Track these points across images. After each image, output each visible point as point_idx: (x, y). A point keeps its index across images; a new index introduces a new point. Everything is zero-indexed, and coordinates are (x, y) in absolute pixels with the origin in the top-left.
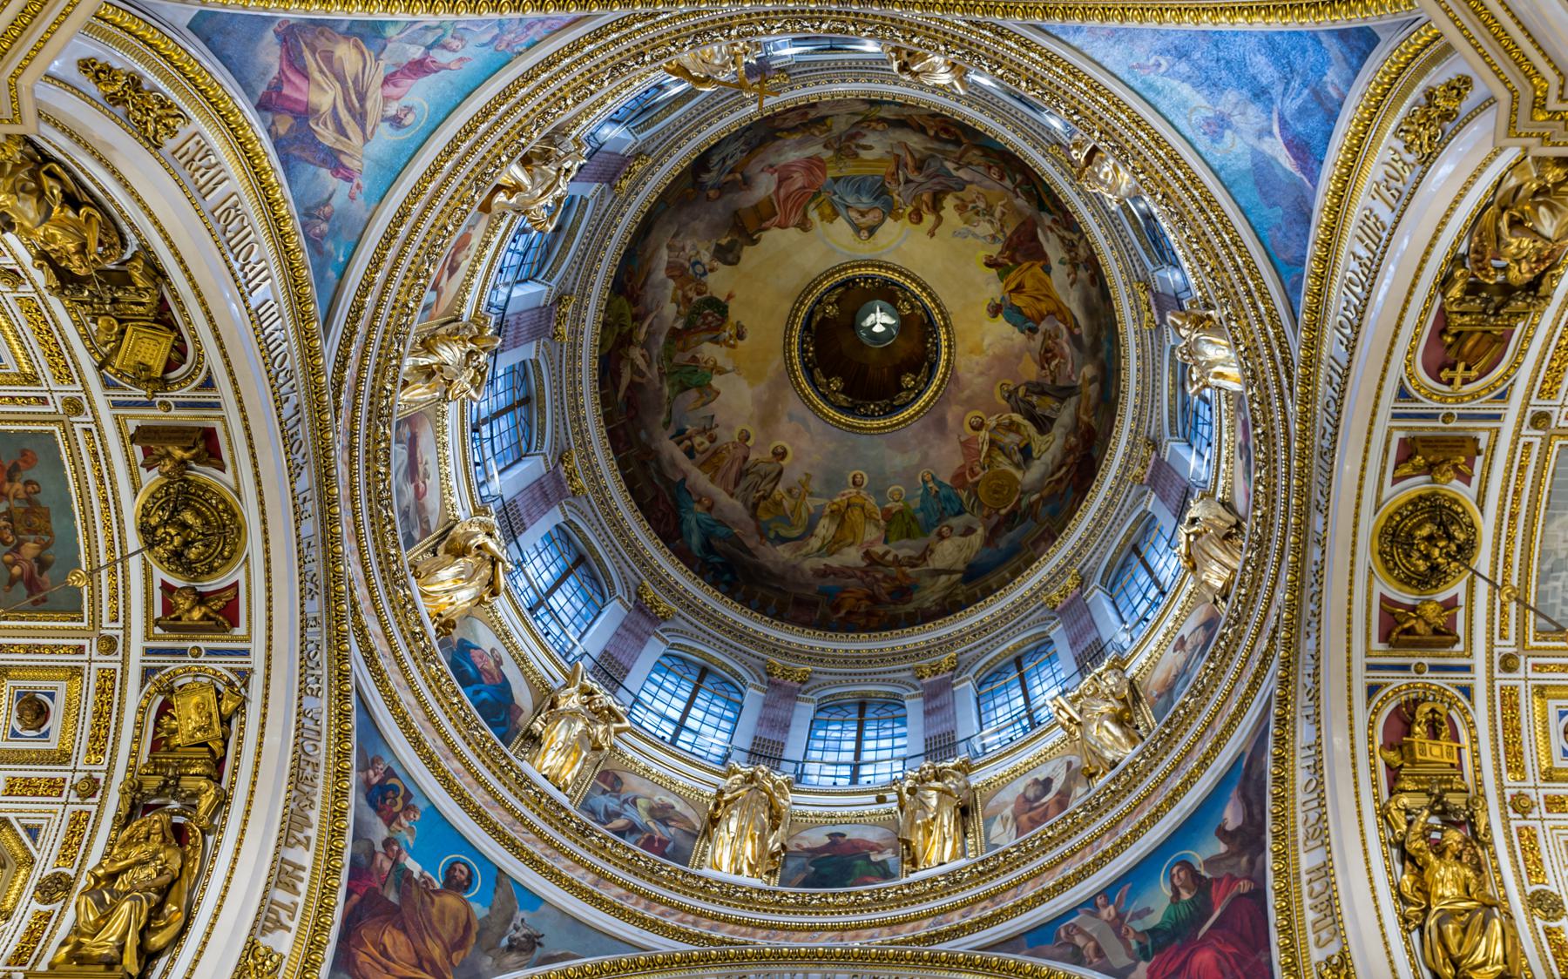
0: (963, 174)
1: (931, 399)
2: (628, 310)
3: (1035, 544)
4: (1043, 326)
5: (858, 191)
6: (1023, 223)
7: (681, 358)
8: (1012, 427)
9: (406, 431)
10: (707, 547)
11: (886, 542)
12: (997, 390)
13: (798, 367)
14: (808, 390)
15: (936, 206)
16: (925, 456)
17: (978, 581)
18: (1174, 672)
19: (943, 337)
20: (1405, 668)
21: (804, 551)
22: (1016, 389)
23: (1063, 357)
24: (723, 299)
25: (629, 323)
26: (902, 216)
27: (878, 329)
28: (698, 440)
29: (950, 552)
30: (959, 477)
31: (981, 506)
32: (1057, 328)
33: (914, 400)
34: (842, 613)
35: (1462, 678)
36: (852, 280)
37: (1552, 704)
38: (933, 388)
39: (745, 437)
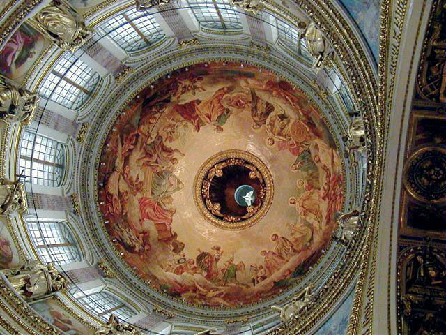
0: (154, 136)
2: (190, 293)
4: (226, 106)
5: (159, 185)
6: (177, 110)
7: (221, 276)
8: (272, 124)
11: (319, 189)
12: (256, 131)
13: (238, 224)
15: (169, 151)
16: (284, 168)
22: (255, 121)
24: (199, 253)
25: (196, 295)
26: (173, 167)
30: (295, 152)
31: (306, 141)
36: (202, 195)
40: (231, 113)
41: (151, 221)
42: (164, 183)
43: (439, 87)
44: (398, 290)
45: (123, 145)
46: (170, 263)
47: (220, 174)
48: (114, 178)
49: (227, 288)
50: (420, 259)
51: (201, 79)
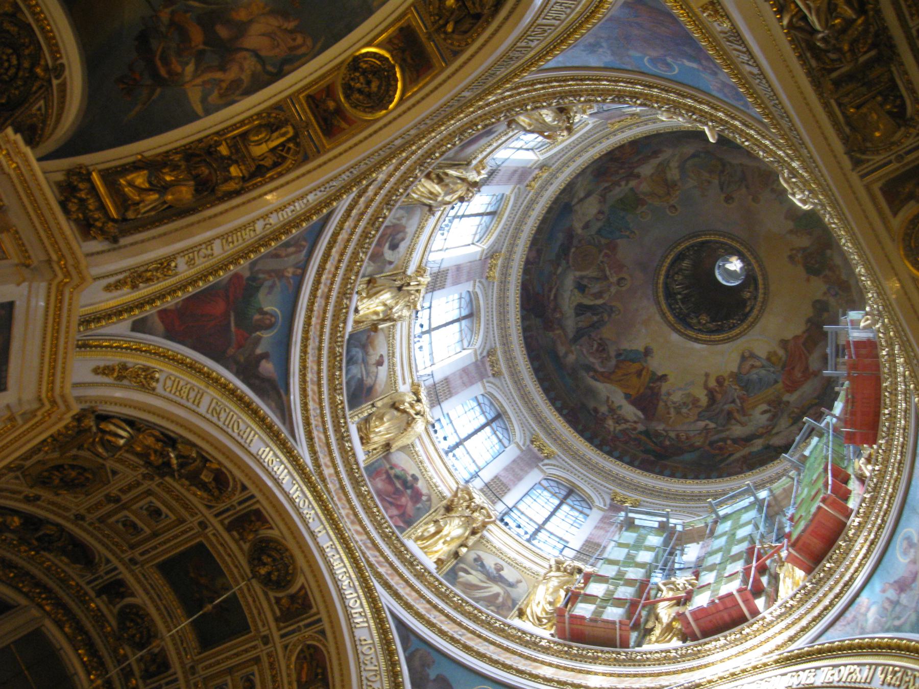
0: (702, 424)
3: (539, 252)
4: (613, 362)
5: (760, 380)
8: (599, 295)
11: (632, 189)
15: (711, 394)
17: (562, 208)
18: (371, 351)
19: (671, 318)
20: (240, 503)
22: (610, 316)
30: (612, 247)
33: (668, 271)
35: (216, 511)
36: (743, 321)
37: (173, 518)
38: (661, 286)
39: (756, 199)
41: (811, 359)
42: (755, 376)
43: (283, 145)
44: (488, 23)
45: (730, 455)
47: (704, 319)
48: (776, 441)
50: (450, 28)
51: (596, 410)
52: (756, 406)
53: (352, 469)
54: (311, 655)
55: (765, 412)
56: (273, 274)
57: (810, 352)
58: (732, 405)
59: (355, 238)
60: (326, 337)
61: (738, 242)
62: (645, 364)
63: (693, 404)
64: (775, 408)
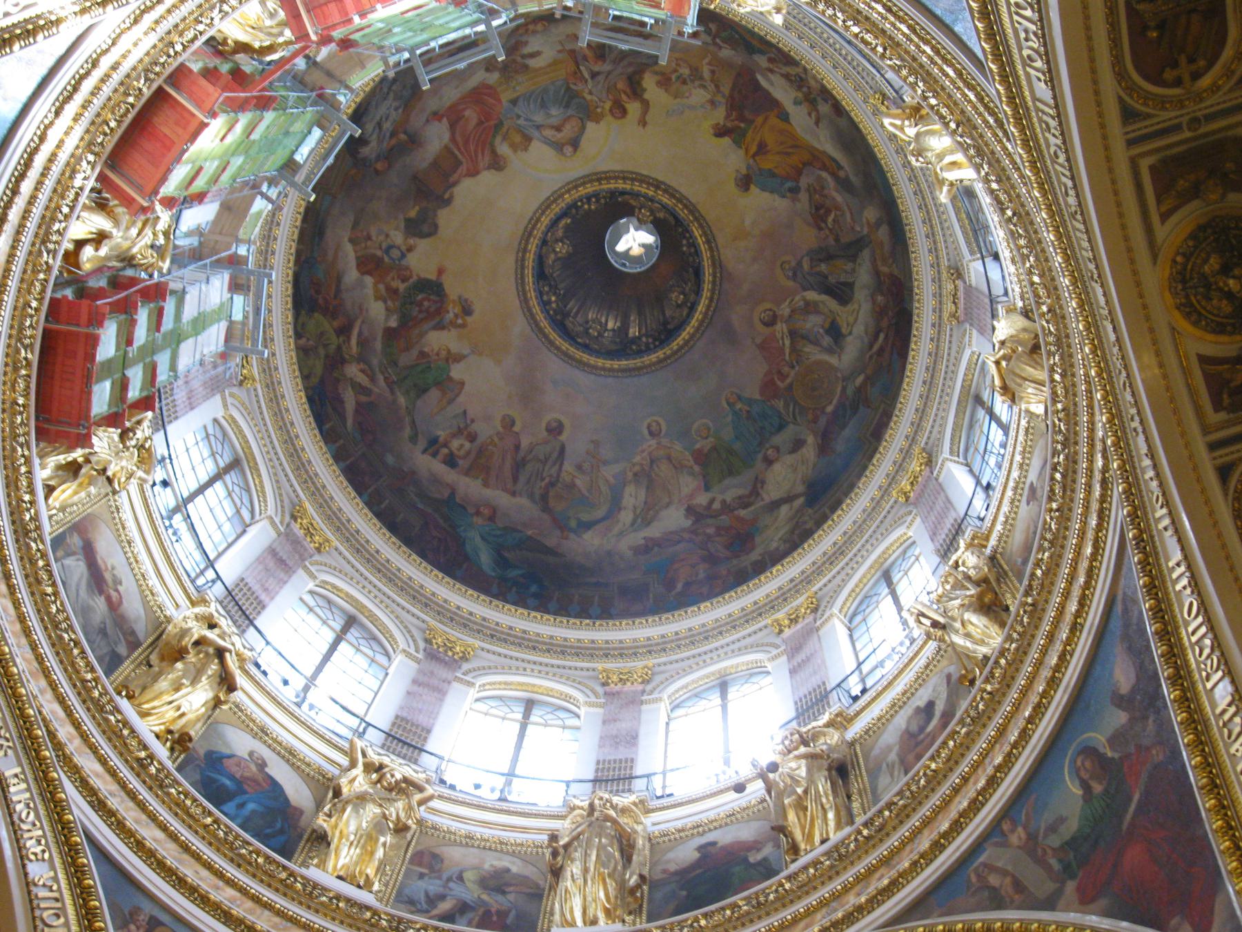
1: (709, 307)
2: (328, 326)
4: (804, 182)
5: (543, 105)
6: (739, 75)
7: (406, 359)
9: (75, 541)
10: (502, 562)
11: (707, 488)
12: (778, 270)
13: (544, 323)
14: (565, 346)
15: (636, 90)
19: (697, 233)
21: (616, 530)
22: (799, 264)
23: (837, 208)
24: (432, 276)
25: (334, 340)
27: (637, 251)
28: (455, 444)
29: (784, 476)
30: (769, 387)
32: (819, 178)
34: (679, 586)
38: (706, 294)
39: (509, 423)
40: (794, 200)
46: (373, 233)
49: (388, 394)
52: (550, 65)
53: (1063, 376)
54: (1175, 65)
55: (532, 55)
56: (1040, 852)
57: (446, 147)
58: (596, 69)
59: (915, 821)
60: (1034, 654)
61: (558, 348)
62: (751, 161)
63: (670, 79)
64: (514, 61)
